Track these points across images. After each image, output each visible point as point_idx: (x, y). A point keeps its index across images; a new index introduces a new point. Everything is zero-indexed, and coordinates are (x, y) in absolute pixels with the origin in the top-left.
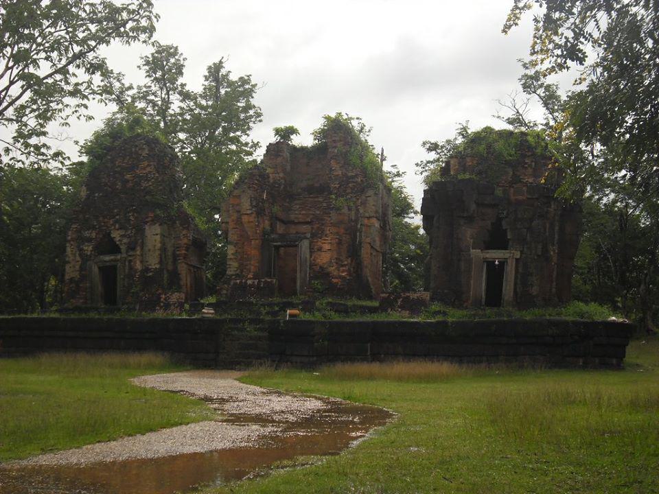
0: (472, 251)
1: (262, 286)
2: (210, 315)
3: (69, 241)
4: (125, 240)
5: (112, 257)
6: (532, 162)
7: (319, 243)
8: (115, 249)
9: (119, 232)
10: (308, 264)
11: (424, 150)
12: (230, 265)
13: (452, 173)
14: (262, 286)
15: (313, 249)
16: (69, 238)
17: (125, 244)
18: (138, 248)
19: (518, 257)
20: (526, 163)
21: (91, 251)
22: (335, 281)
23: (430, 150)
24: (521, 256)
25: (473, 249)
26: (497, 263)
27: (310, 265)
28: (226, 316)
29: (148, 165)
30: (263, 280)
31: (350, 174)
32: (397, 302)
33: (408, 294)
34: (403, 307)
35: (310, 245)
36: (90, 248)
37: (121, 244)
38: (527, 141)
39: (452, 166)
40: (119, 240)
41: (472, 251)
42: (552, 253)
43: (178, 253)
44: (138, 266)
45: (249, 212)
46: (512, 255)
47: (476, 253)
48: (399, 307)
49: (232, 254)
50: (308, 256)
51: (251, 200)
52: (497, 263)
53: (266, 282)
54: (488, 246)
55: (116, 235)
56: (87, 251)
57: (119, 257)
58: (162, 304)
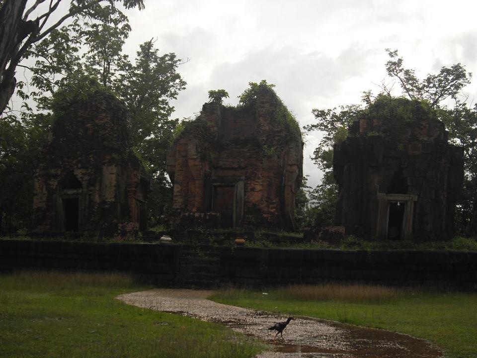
0: (379, 194)
1: (208, 218)
2: (168, 242)
3: (36, 177)
4: (86, 178)
5: (75, 191)
6: (427, 124)
7: (252, 185)
8: (76, 184)
9: (81, 170)
10: (243, 202)
11: (313, 116)
12: (176, 200)
13: (361, 131)
14: (208, 218)
15: (246, 189)
16: (37, 174)
18: (97, 184)
19: (416, 200)
20: (422, 125)
22: (265, 215)
23: (317, 116)
24: (418, 200)
25: (379, 192)
26: (399, 204)
27: (245, 203)
28: (179, 243)
29: (106, 117)
30: (209, 214)
31: (276, 129)
32: (318, 234)
33: (327, 228)
34: (323, 239)
35: (245, 185)
36: (56, 183)
37: (83, 181)
38: (422, 108)
39: (361, 126)
40: (82, 178)
41: (379, 194)
42: (442, 197)
43: (129, 189)
44: (97, 199)
45: (195, 157)
46: (411, 198)
47: (382, 196)
48: (320, 239)
49: (178, 192)
50: (243, 196)
51: (196, 148)
52: (399, 204)
53: (210, 215)
54: (389, 192)
55: (78, 173)
56: (53, 185)
57: (80, 191)
58: (119, 232)
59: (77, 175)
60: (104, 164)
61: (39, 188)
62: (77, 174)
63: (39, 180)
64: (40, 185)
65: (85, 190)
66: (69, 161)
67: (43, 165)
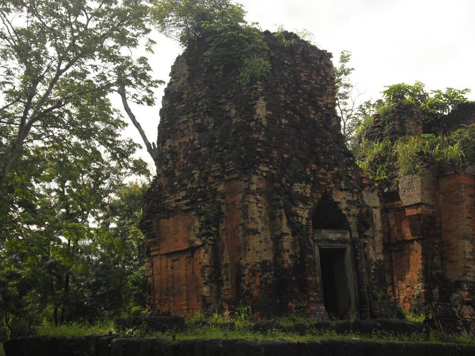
4: (354, 210)
5: (339, 235)
12: (469, 268)
16: (254, 187)
17: (354, 215)
21: (307, 219)
36: (306, 215)
37: (350, 215)
40: (347, 209)
59: (339, 203)
60: (363, 187)
61: (260, 217)
62: (339, 200)
64: (260, 212)
65: (355, 235)
66: (322, 171)
67: (266, 169)
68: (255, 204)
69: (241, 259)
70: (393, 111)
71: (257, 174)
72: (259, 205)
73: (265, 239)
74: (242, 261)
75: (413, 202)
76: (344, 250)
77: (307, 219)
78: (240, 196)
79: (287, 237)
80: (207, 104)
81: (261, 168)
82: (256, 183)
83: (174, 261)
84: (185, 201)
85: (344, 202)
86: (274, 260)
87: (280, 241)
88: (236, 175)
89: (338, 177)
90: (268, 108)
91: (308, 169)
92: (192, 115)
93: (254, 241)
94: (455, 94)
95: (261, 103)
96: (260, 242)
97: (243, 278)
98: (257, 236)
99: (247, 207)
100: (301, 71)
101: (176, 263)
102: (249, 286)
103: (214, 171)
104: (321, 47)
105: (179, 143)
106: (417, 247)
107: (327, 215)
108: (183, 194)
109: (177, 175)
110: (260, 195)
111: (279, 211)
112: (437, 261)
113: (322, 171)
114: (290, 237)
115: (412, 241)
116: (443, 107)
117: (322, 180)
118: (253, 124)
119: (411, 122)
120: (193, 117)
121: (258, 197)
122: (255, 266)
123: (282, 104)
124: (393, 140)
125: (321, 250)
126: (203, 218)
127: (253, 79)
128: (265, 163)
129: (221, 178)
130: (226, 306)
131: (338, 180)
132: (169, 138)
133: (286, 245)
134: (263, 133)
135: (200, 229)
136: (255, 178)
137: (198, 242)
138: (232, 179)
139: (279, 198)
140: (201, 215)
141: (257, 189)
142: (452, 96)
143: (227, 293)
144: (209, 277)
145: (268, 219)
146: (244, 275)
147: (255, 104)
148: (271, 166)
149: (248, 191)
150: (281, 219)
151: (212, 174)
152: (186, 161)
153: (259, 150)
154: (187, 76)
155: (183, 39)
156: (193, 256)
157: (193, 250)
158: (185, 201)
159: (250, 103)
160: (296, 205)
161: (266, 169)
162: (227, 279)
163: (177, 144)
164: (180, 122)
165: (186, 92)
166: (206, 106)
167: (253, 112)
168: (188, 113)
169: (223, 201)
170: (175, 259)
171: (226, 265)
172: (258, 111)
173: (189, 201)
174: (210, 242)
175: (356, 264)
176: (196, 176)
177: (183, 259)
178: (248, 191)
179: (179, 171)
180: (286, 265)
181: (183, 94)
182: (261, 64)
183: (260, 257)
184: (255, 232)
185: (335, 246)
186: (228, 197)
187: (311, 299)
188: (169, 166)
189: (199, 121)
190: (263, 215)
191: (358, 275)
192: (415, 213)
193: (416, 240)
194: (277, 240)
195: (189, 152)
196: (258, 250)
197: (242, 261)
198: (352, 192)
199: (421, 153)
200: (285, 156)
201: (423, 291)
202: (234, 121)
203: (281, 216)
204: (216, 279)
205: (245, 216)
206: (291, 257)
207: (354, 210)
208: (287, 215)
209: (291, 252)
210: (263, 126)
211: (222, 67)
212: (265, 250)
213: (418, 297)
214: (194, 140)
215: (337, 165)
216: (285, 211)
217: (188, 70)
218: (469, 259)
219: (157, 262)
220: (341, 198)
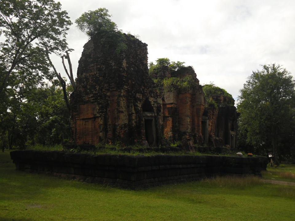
4: (156, 105)
5: (151, 114)
16: (122, 94)
17: (156, 107)
36: (140, 106)
47: (230, 131)
63: (124, 100)
64: (124, 104)
65: (156, 114)
67: (126, 87)
68: (122, 101)
69: (116, 122)
70: (161, 68)
71: (123, 89)
72: (124, 101)
73: (126, 115)
74: (116, 123)
75: (170, 103)
76: (152, 120)
77: (141, 108)
78: (116, 98)
79: (134, 115)
80: (103, 60)
81: (125, 87)
82: (123, 93)
83: (86, 122)
84: (92, 98)
85: (152, 101)
86: (129, 123)
87: (131, 116)
88: (115, 89)
89: (151, 92)
90: (127, 63)
91: (141, 88)
92: (95, 64)
93: (122, 116)
94: (180, 63)
95: (125, 61)
96: (124, 116)
97: (117, 130)
98: (123, 113)
99: (120, 102)
100: (138, 50)
101: (86, 123)
102: (119, 133)
103: (105, 87)
104: (143, 42)
105: (89, 75)
106: (170, 119)
107: (147, 107)
108: (92, 95)
109: (88, 87)
110: (124, 97)
111: (131, 104)
112: (177, 124)
113: (146, 89)
114: (135, 115)
115: (168, 117)
116: (175, 68)
117: (146, 93)
118: (121, 69)
119: (167, 73)
120: (96, 65)
121: (123, 98)
122: (122, 125)
123: (131, 62)
124: (162, 79)
125: (145, 119)
126: (100, 106)
127: (122, 52)
128: (126, 85)
129: (108, 90)
130: (110, 141)
131: (151, 93)
132: (85, 72)
133: (134, 118)
134: (125, 73)
135: (99, 110)
136: (122, 91)
137: (98, 115)
138: (113, 91)
139: (131, 99)
140: (100, 104)
141: (123, 95)
142: (179, 64)
143: (110, 135)
144: (103, 129)
145: (126, 107)
146: (117, 129)
147: (122, 61)
148: (128, 86)
149: (120, 96)
150: (132, 107)
151: (104, 88)
152: (92, 82)
153: (124, 80)
154: (93, 48)
155: (89, 34)
156: (95, 121)
157: (95, 118)
158: (92, 98)
159: (120, 61)
160: (137, 102)
161: (126, 87)
162: (110, 130)
163: (88, 75)
164: (90, 66)
165: (93, 54)
166: (102, 61)
167: (122, 64)
168: (94, 63)
169: (109, 99)
170: (86, 121)
171: (110, 125)
172: (124, 64)
173: (94, 98)
174: (103, 115)
175: (156, 125)
176: (97, 88)
177: (90, 121)
178: (120, 96)
179: (89, 86)
180: (133, 125)
181: (91, 55)
182: (123, 46)
183: (124, 122)
184: (122, 112)
185: (150, 118)
186: (111, 98)
187: (143, 138)
188: (85, 84)
189: (99, 66)
190: (125, 105)
191: (157, 129)
192: (170, 107)
193: (170, 116)
194: (130, 115)
195: (94, 78)
196: (123, 119)
197: (116, 123)
198: (155, 98)
199: (172, 84)
200: (133, 83)
201: (172, 135)
202: (114, 67)
203: (132, 106)
204: (105, 130)
205: (119, 106)
206: (135, 122)
207: (156, 105)
208: (134, 106)
209: (135, 120)
210: (125, 70)
211: (108, 46)
212: (125, 119)
213: (170, 137)
214: (96, 74)
215: (150, 87)
216: (134, 104)
217: (94, 46)
218: (189, 124)
219: (78, 122)
220: (151, 100)
